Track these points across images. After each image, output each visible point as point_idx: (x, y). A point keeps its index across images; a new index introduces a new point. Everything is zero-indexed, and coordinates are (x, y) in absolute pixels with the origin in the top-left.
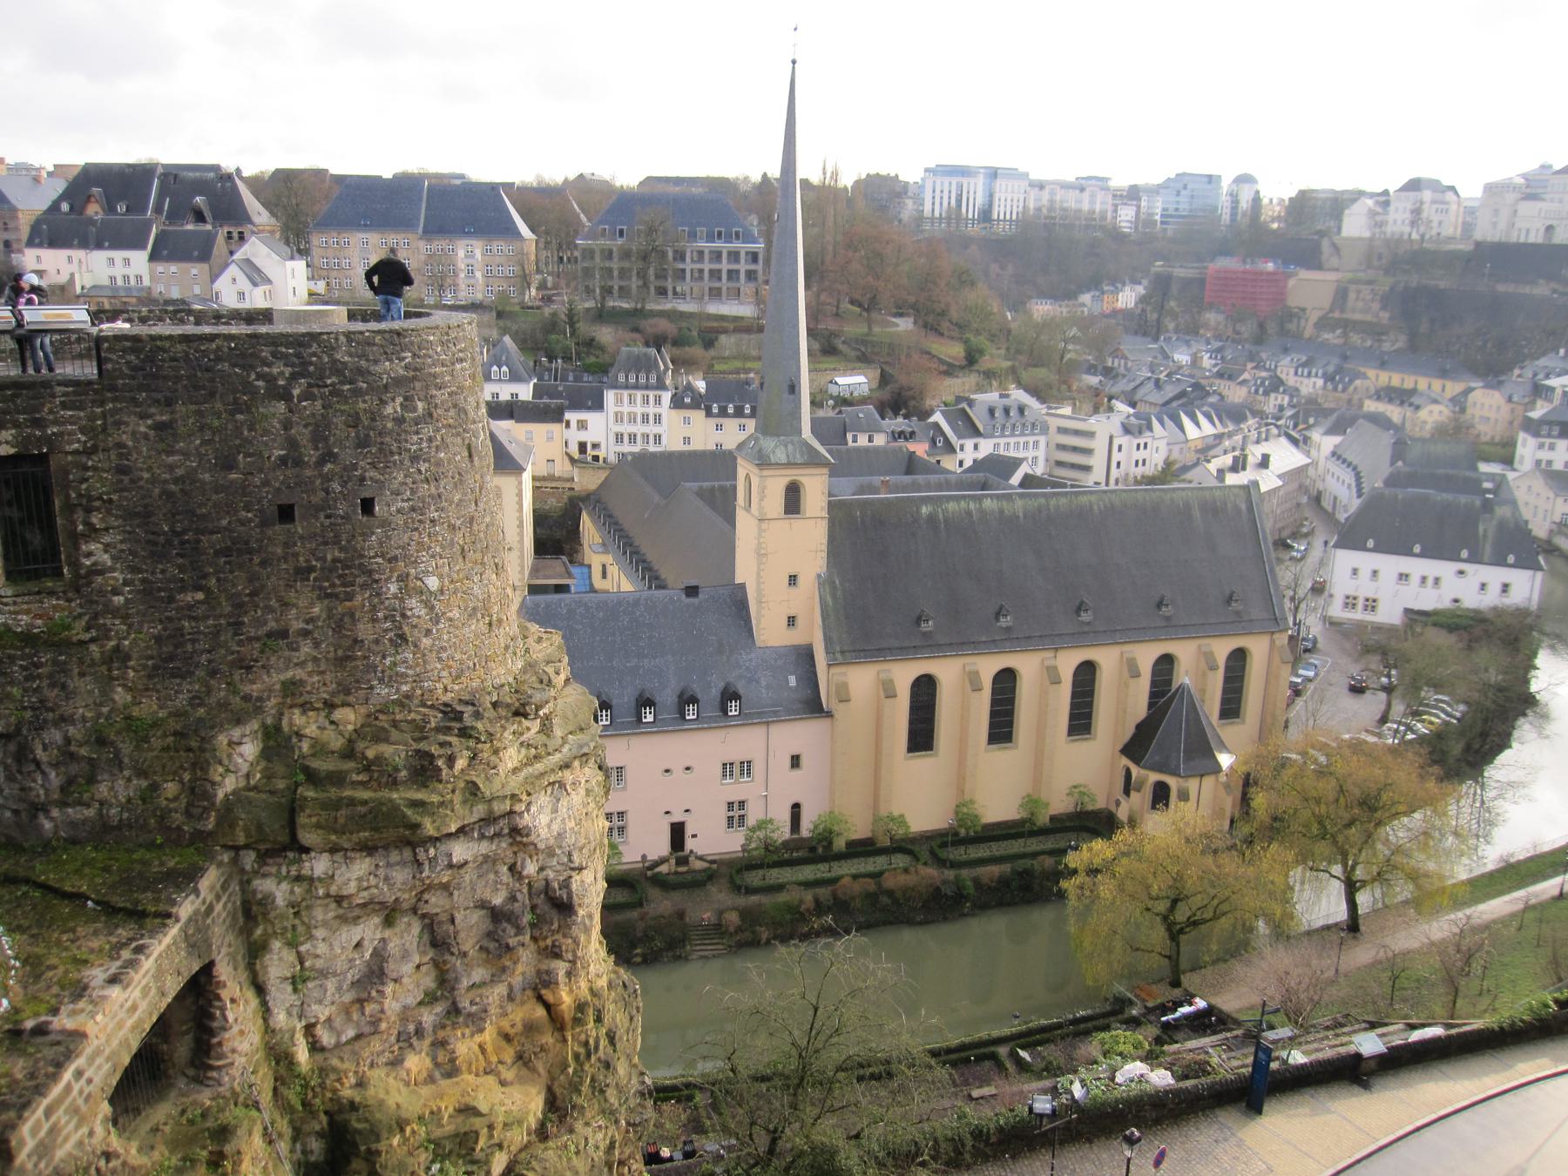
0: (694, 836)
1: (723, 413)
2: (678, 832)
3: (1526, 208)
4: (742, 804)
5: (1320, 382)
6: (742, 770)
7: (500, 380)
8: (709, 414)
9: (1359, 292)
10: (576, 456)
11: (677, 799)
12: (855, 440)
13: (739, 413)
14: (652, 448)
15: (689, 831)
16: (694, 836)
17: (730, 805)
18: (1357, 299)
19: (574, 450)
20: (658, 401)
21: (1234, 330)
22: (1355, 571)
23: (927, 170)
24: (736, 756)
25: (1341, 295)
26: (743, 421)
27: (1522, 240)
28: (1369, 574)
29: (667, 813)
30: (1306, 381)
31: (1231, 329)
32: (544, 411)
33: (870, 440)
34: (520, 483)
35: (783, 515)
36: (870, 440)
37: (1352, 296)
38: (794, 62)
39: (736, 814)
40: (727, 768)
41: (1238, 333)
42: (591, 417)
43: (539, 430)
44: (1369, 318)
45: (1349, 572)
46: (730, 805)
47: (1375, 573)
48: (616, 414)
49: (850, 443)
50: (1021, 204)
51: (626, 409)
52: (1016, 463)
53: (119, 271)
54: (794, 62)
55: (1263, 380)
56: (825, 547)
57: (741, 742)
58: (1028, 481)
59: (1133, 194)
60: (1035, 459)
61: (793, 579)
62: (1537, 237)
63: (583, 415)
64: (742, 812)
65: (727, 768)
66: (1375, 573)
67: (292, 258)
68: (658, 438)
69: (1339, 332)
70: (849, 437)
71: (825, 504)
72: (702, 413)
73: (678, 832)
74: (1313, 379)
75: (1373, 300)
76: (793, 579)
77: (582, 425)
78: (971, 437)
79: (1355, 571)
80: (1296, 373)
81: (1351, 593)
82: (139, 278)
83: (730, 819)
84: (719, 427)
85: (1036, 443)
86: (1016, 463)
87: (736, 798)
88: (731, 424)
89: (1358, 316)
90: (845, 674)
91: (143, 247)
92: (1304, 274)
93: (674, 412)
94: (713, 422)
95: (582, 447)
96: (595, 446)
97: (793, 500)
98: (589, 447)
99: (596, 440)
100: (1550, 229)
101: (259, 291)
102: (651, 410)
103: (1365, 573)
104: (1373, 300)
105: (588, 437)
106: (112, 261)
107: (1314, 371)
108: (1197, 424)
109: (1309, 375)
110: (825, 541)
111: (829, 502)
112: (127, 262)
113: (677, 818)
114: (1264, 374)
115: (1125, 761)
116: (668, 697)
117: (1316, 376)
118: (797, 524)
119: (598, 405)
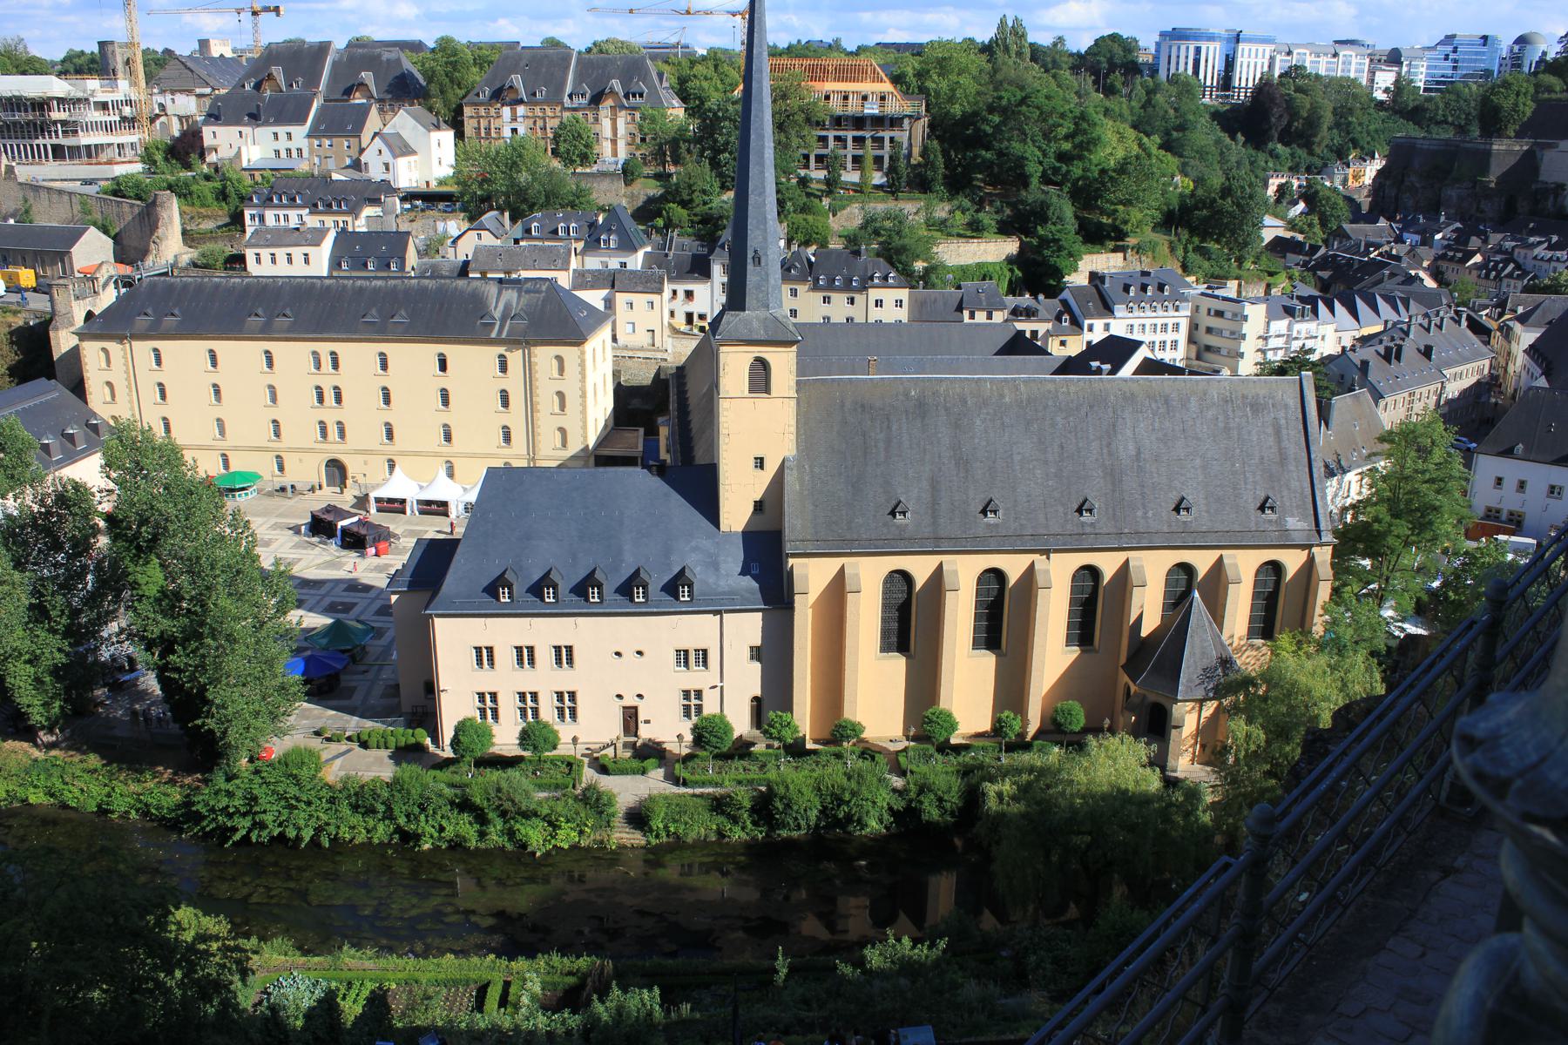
0: (647, 722)
1: (830, 286)
2: (631, 718)
4: (699, 694)
6: (697, 658)
8: (816, 287)
10: (684, 327)
11: (631, 680)
12: (972, 316)
13: (847, 287)
15: (642, 717)
16: (647, 722)
17: (687, 694)
19: (680, 323)
21: (1478, 208)
22: (1499, 481)
23: (1163, 34)
24: (691, 645)
28: (1515, 484)
29: (619, 696)
31: (1475, 206)
32: (647, 283)
33: (990, 317)
34: (583, 353)
35: (746, 393)
36: (990, 317)
39: (691, 700)
40: (683, 657)
41: (1482, 212)
42: (700, 289)
43: (640, 299)
45: (1492, 482)
46: (687, 694)
47: (1522, 485)
49: (966, 319)
50: (1266, 69)
52: (1134, 345)
53: (283, 144)
55: (1497, 263)
56: (793, 429)
57: (696, 629)
58: (1150, 367)
59: (1394, 58)
60: (1175, 344)
61: (760, 463)
63: (689, 287)
64: (698, 702)
65: (683, 657)
66: (1522, 485)
67: (438, 127)
70: (966, 313)
71: (793, 384)
73: (631, 718)
76: (760, 463)
77: (689, 295)
78: (1100, 316)
79: (1499, 481)
81: (1493, 504)
84: (826, 300)
85: (1176, 327)
86: (1134, 345)
87: (692, 686)
88: (840, 299)
90: (806, 565)
91: (300, 119)
94: (820, 295)
95: (689, 318)
96: (702, 317)
97: (761, 377)
98: (696, 318)
99: (702, 311)
101: (402, 163)
103: (1510, 484)
105: (696, 307)
108: (1375, 309)
110: (793, 422)
111: (798, 383)
113: (630, 701)
114: (1498, 258)
116: (656, 581)
118: (762, 402)
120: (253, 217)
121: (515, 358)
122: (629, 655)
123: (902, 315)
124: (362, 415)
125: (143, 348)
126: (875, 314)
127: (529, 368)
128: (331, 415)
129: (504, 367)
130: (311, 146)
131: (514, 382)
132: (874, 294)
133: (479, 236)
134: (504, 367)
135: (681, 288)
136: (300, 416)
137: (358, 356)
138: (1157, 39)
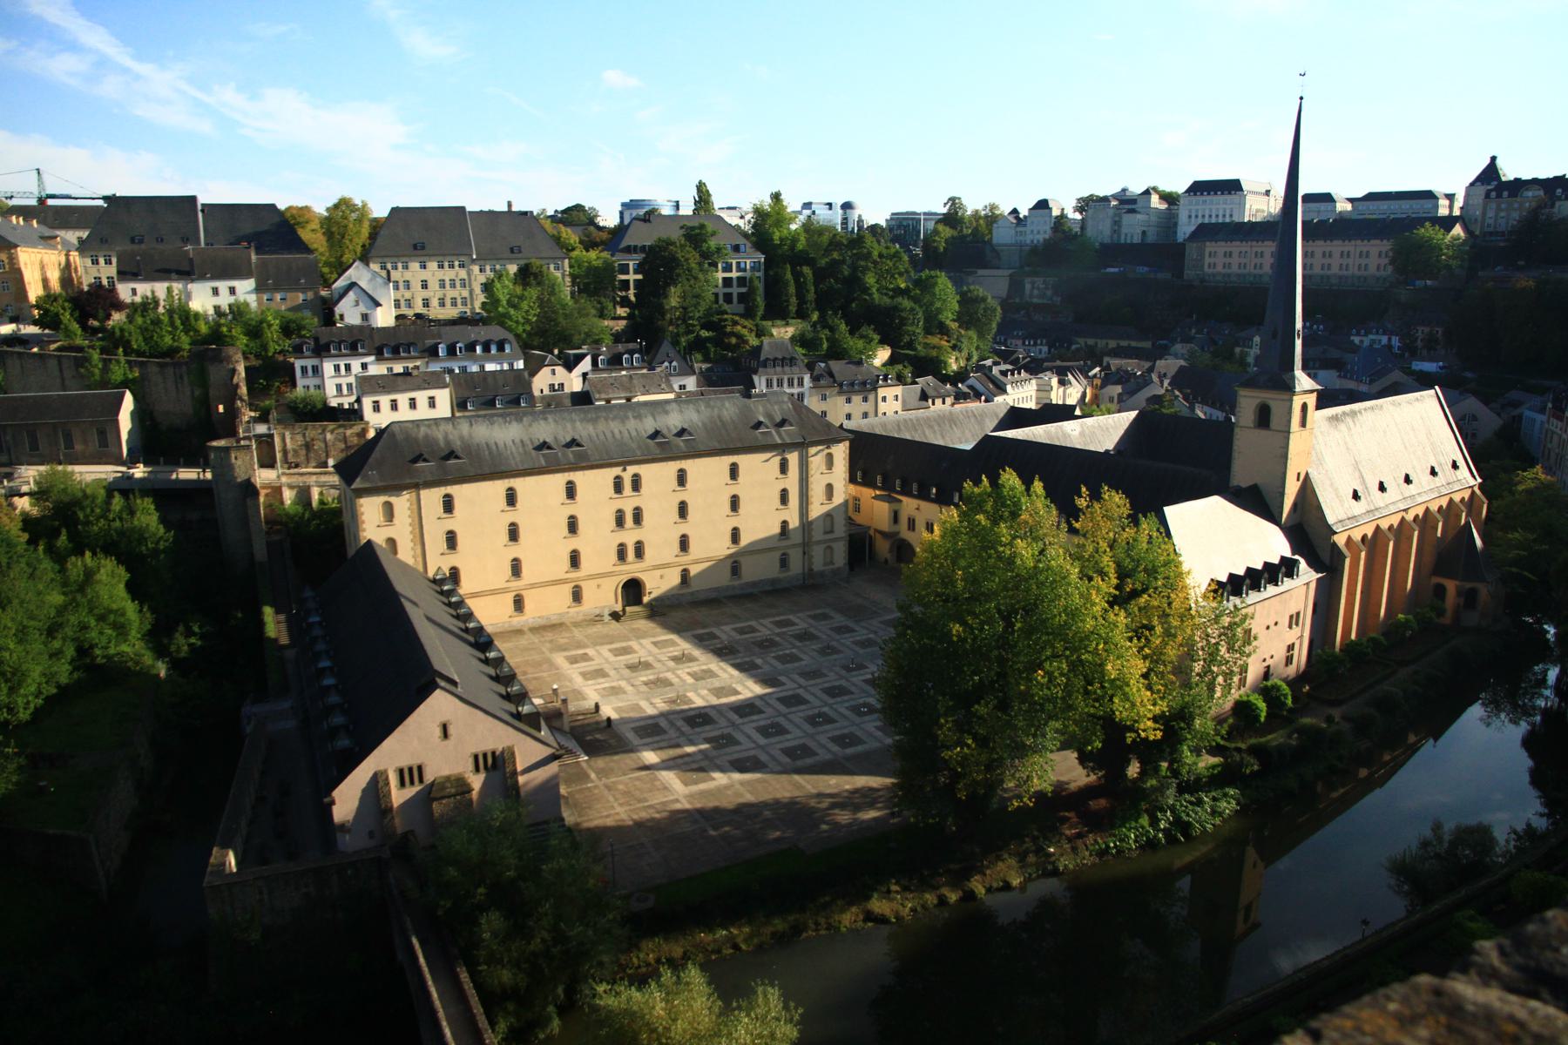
3: (1128, 219)
5: (1045, 349)
9: (1033, 283)
12: (933, 404)
18: (1033, 288)
20: (801, 383)
23: (623, 205)
25: (1015, 285)
27: (1129, 241)
30: (1033, 349)
36: (944, 403)
37: (1028, 286)
38: (1301, 98)
44: (1045, 301)
54: (1301, 98)
62: (1137, 239)
69: (1022, 312)
72: (836, 389)
74: (1038, 347)
75: (1047, 288)
80: (1024, 343)
83: (1287, 658)
88: (857, 399)
89: (1035, 300)
92: (981, 272)
100: (1144, 233)
104: (1047, 288)
106: (216, 292)
107: (1039, 342)
109: (1035, 344)
112: (232, 291)
115: (1435, 580)
117: (1041, 344)
120: (304, 370)
121: (793, 458)
122: (1272, 627)
123: (898, 406)
124: (659, 534)
125: (432, 498)
128: (630, 537)
129: (784, 468)
131: (792, 482)
133: (553, 372)
134: (784, 468)
136: (598, 542)
137: (657, 476)
138: (620, 208)
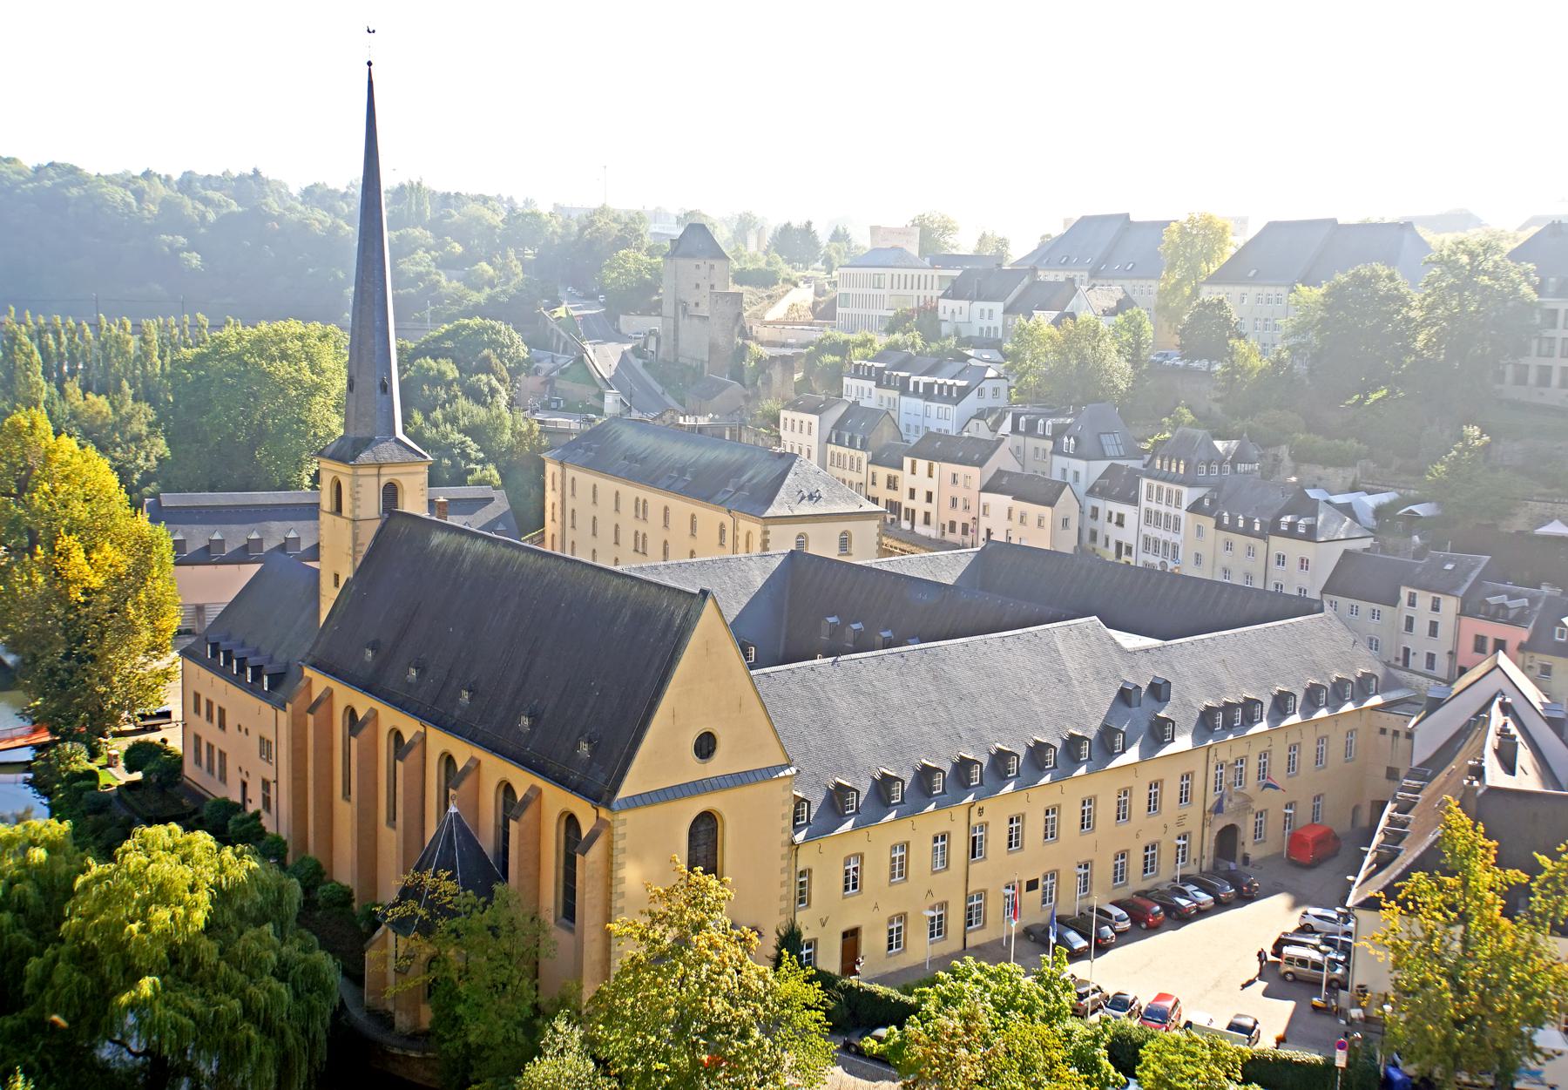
7: (1068, 455)
14: (1171, 565)
20: (1178, 504)
26: (1252, 540)
48: (1148, 511)
51: (1154, 506)
54: (370, 64)
68: (1175, 547)
76: (337, 577)
77: (1120, 523)
82: (996, 329)
93: (1190, 515)
94: (1223, 535)
102: (1173, 511)
113: (246, 779)
119: (1134, 501)
126: (1277, 574)
127: (735, 538)
130: (1005, 326)
132: (1278, 544)
135: (1116, 508)
